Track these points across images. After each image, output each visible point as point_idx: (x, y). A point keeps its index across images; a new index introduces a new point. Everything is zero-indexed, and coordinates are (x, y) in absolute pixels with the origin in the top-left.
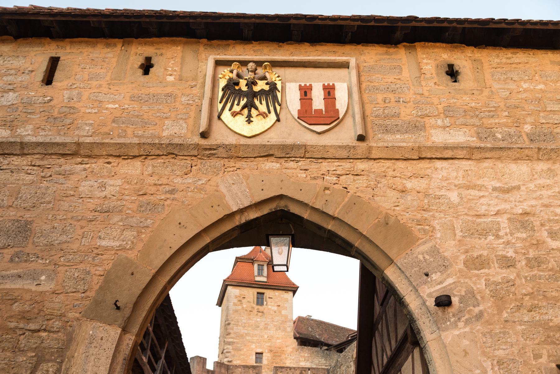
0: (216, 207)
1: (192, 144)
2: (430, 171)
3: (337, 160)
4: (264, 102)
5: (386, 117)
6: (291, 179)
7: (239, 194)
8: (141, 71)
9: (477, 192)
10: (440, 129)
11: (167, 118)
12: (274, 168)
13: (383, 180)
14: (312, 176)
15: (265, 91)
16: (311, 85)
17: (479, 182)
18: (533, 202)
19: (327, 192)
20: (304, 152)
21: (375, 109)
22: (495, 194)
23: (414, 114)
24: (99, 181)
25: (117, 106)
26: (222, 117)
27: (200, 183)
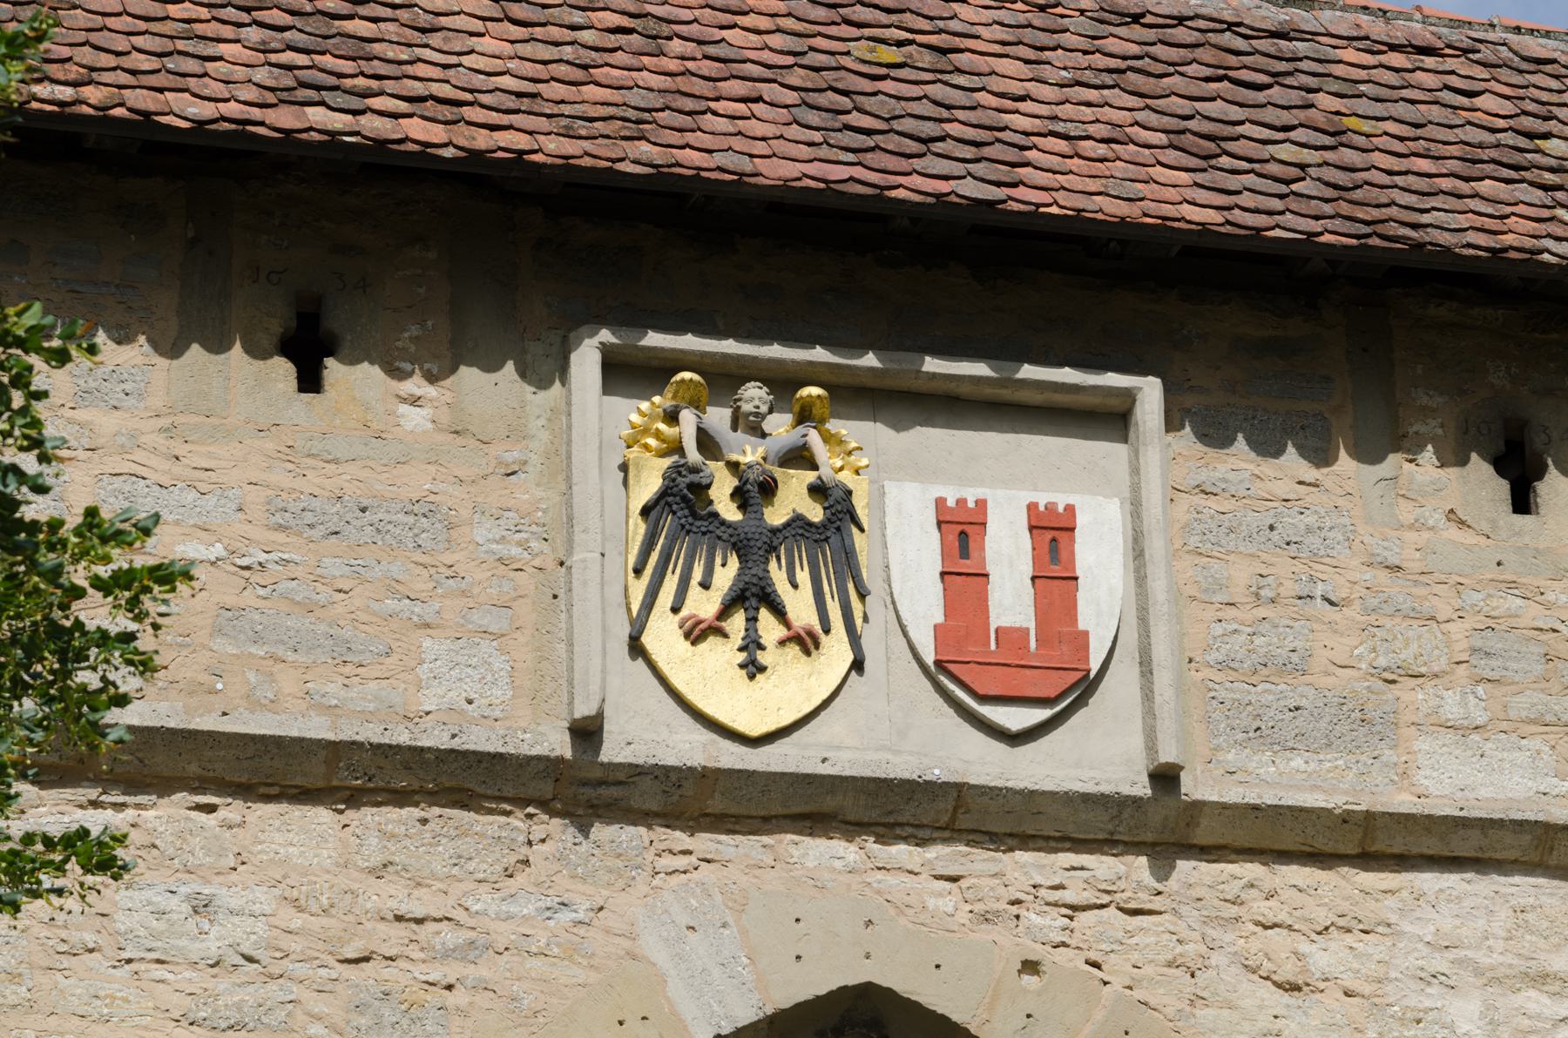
0: (633, 1023)
1: (539, 758)
2: (1391, 902)
3: (1068, 845)
4: (803, 576)
5: (1265, 668)
6: (902, 921)
7: (716, 972)
8: (282, 370)
9: (1545, 1000)
10: (1450, 736)
11: (428, 626)
12: (838, 864)
13: (1229, 937)
14: (978, 907)
15: (810, 524)
16: (981, 504)
19: (1029, 980)
20: (950, 808)
21: (1218, 629)
23: (1360, 657)
24: (183, 890)
25: (218, 550)
26: (647, 640)
27: (565, 916)
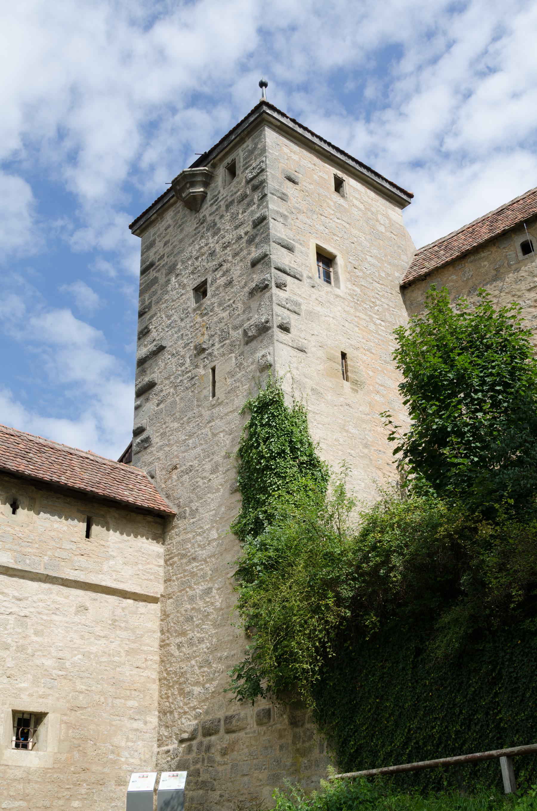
17: (6, 591)
18: (32, 610)
22: (13, 600)
